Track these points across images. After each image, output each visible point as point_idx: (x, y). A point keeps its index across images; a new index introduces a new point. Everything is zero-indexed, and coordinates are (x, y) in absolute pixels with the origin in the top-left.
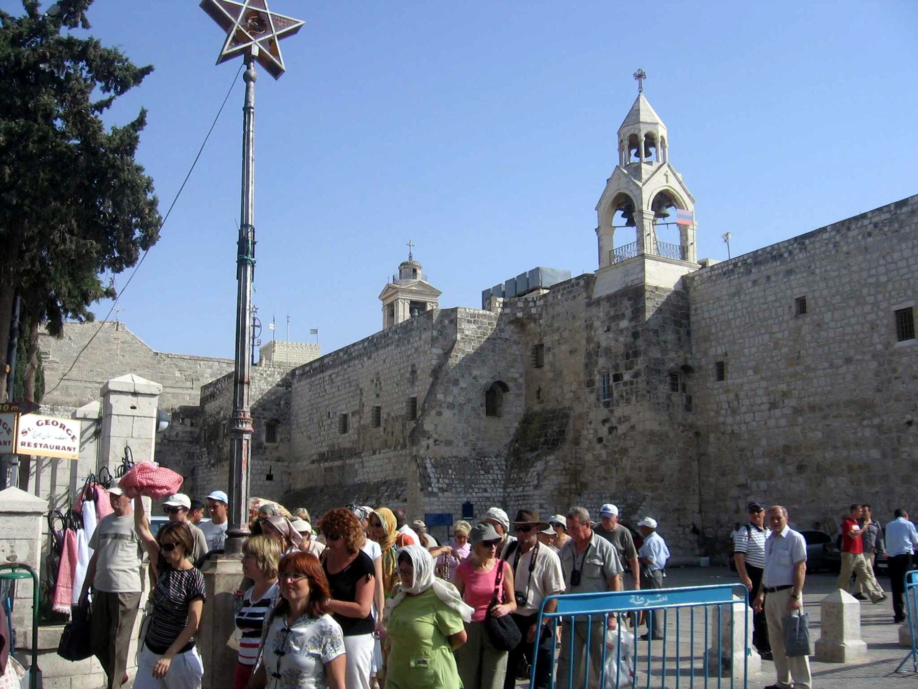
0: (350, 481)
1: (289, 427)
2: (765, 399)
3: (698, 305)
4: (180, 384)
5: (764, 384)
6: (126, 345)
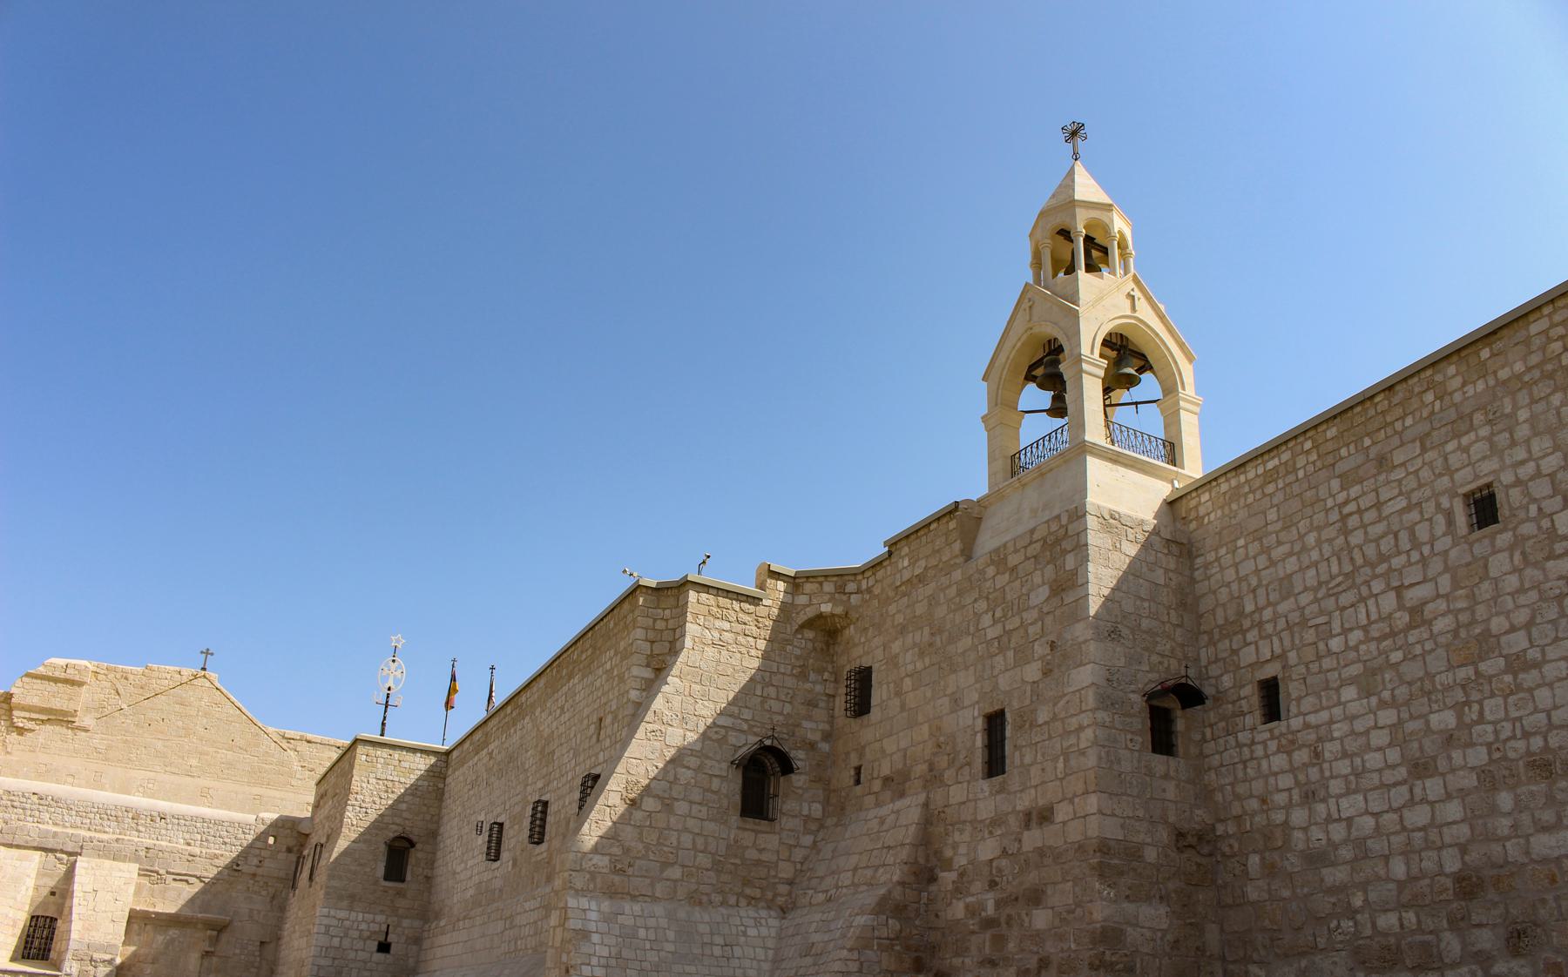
2: (1394, 755)
3: (1211, 557)
5: (1388, 717)
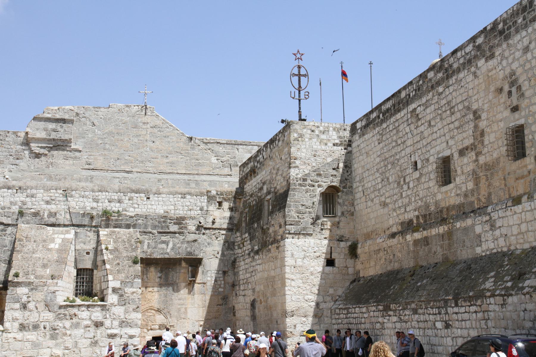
0: (464, 254)
1: (351, 197)
4: (217, 171)
6: (155, 130)
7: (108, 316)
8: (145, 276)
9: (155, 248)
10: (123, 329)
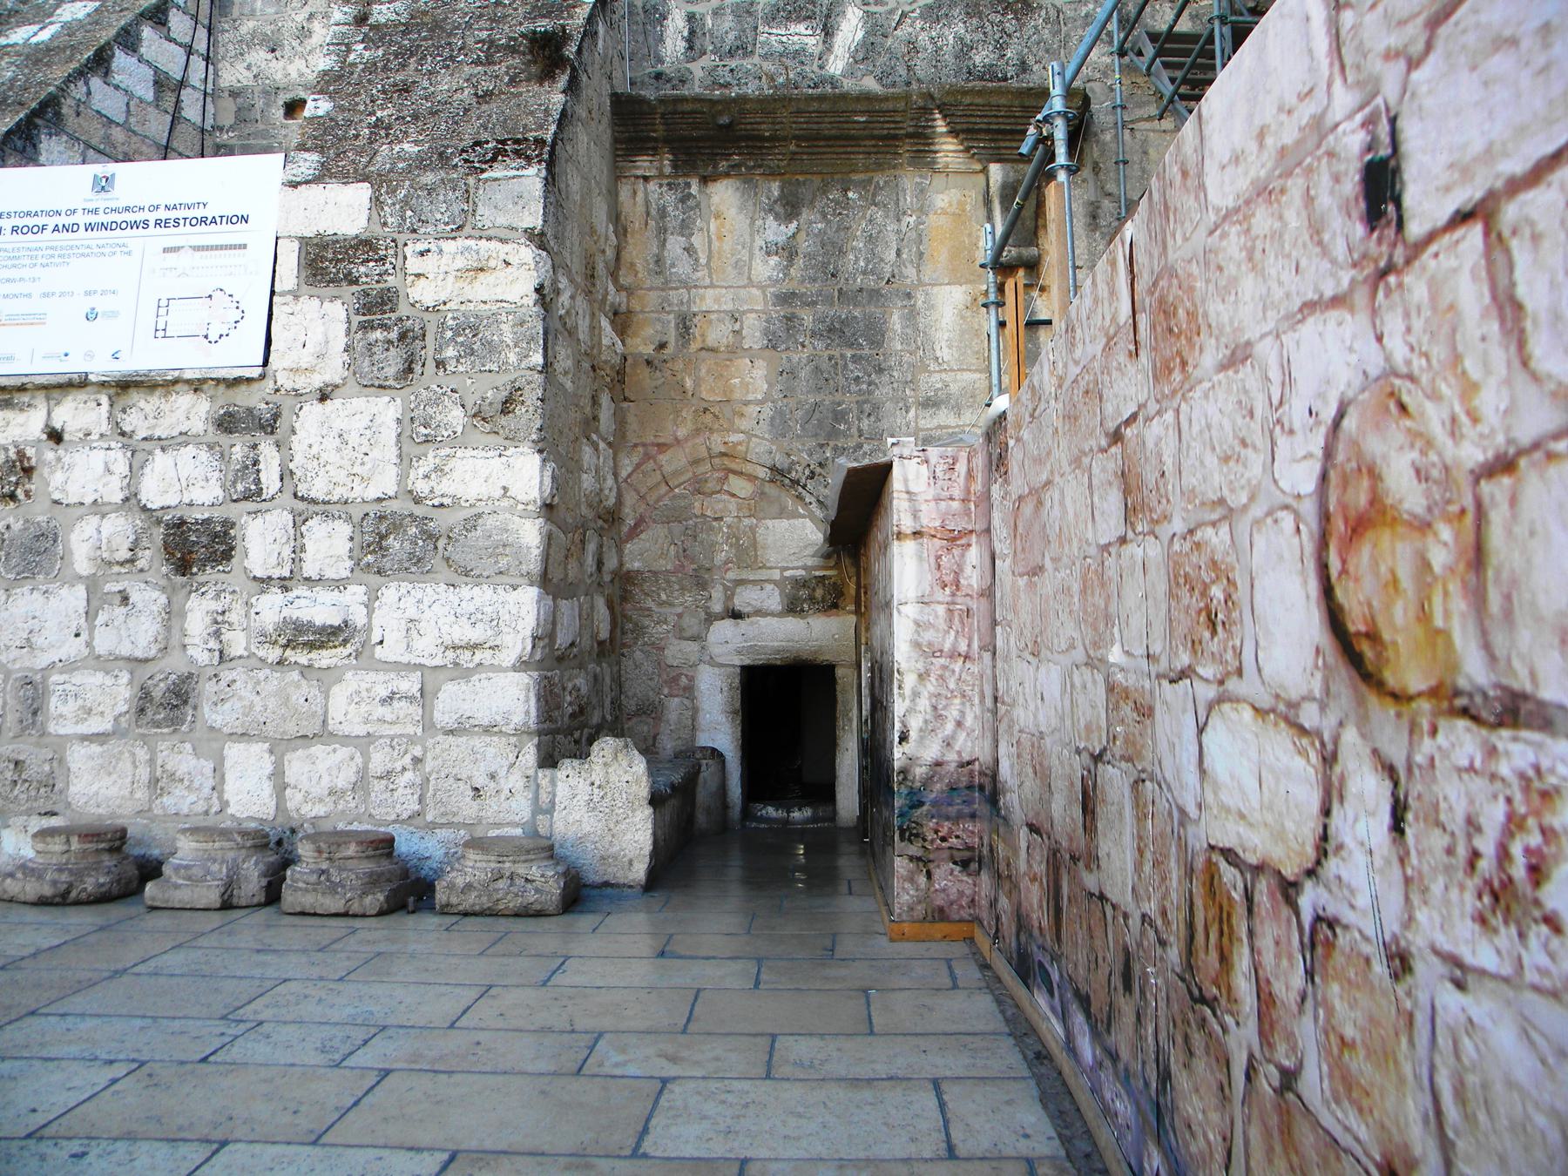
7: (270, 479)
8: (675, 244)
9: (741, 48)
10: (390, 593)
